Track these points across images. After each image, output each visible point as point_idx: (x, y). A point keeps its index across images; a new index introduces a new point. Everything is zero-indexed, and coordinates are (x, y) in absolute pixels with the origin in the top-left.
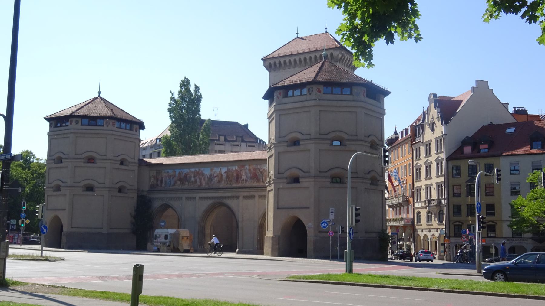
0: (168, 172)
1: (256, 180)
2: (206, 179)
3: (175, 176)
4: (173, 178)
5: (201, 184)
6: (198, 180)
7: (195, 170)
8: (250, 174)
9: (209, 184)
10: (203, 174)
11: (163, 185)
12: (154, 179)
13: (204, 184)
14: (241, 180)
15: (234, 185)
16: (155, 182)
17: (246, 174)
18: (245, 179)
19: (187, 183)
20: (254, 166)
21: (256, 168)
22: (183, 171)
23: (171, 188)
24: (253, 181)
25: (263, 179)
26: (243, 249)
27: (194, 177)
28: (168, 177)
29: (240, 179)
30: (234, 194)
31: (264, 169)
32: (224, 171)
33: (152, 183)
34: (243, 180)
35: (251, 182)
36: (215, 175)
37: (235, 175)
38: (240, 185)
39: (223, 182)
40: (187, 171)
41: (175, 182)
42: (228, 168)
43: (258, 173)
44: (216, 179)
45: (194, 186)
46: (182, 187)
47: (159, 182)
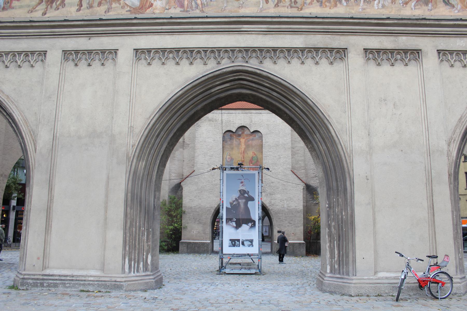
26: (381, 275)
45: (108, 11)
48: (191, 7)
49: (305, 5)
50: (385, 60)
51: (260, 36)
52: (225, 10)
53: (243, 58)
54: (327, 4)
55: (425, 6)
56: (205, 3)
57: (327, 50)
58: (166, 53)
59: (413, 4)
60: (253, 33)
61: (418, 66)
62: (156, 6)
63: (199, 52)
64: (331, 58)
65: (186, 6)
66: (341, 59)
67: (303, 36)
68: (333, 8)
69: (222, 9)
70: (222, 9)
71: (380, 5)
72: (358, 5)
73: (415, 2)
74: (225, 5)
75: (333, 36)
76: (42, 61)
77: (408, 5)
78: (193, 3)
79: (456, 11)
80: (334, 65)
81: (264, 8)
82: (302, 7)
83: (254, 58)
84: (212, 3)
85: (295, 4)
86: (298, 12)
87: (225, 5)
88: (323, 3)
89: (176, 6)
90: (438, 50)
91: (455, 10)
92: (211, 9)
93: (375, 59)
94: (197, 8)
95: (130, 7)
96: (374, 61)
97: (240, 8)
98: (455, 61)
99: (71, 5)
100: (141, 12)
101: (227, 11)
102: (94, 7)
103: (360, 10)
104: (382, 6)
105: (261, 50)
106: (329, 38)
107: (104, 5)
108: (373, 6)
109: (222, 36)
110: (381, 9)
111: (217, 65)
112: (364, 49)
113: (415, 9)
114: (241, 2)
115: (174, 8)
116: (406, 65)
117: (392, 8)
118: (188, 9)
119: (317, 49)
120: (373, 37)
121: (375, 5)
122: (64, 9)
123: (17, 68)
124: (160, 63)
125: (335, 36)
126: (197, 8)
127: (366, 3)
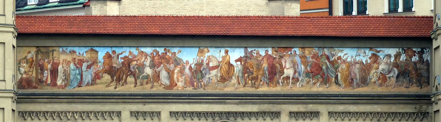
0: (74, 52)
1: (321, 80)
2: (187, 71)
3: (95, 62)
4: (89, 67)
5: (173, 84)
6: (164, 74)
7: (154, 51)
8: (306, 68)
9: (195, 83)
10: (177, 62)
11: (59, 82)
12: (30, 67)
13: (180, 84)
14: (282, 78)
15: (264, 89)
16: (34, 75)
17: (294, 64)
18: (291, 77)
19: (131, 79)
20: (316, 50)
21: (320, 55)
22: (117, 53)
23: (84, 89)
24: (312, 81)
25: (336, 77)
27: (153, 66)
28: (75, 65)
29: (278, 76)
30: (266, 107)
31: (339, 58)
32: (237, 57)
33: (24, 76)
34: (288, 78)
35: (308, 83)
36: (211, 65)
37: (265, 65)
38: (278, 89)
39: (234, 80)
40: (130, 52)
41: (97, 76)
42: (246, 52)
43: (325, 64)
44: (214, 72)
45: (152, 87)
46: (116, 88)
47: (47, 74)
48: (198, 87)
49: (260, 86)
50: (301, 117)
51: (235, 106)
52: (216, 88)
53: (227, 117)
54: (272, 85)
55: (325, 85)
56: (206, 84)
57: (270, 113)
58: (186, 114)
59: (318, 84)
60: (232, 104)
61: (318, 120)
62: (179, 85)
63: (204, 113)
64: (272, 117)
65: (195, 86)
66: (277, 117)
67: (258, 105)
68: (275, 87)
69: (215, 88)
70: (215, 88)
71: (300, 85)
72: (288, 85)
73: (319, 83)
74: (217, 86)
75: (273, 105)
76: (118, 116)
77: (316, 85)
78: (199, 84)
79: (341, 88)
80: (273, 120)
81: (238, 87)
82: (258, 87)
83: (232, 117)
84: (209, 84)
85: (254, 85)
86: (256, 90)
87: (217, 86)
88: (269, 84)
89: (190, 86)
90: (328, 112)
91: (341, 88)
92: (209, 88)
93: (295, 117)
94: (201, 87)
95: (164, 85)
96: (295, 118)
97: (225, 87)
98: (338, 117)
99: (131, 83)
100: (171, 89)
101: (218, 89)
102: (144, 85)
103: (289, 88)
104: (301, 86)
105: (236, 113)
106: (271, 106)
107: (150, 84)
108: (296, 86)
109: (216, 105)
110: (301, 87)
111: (213, 121)
112: (289, 112)
113: (319, 87)
114: (225, 84)
115: (189, 87)
116: (311, 120)
117: (307, 87)
118: (197, 88)
119: (265, 113)
120: (295, 105)
121: (298, 85)
122: (126, 86)
123: (104, 120)
124: (183, 119)
125: (274, 105)
126: (201, 87)
127: (293, 84)
